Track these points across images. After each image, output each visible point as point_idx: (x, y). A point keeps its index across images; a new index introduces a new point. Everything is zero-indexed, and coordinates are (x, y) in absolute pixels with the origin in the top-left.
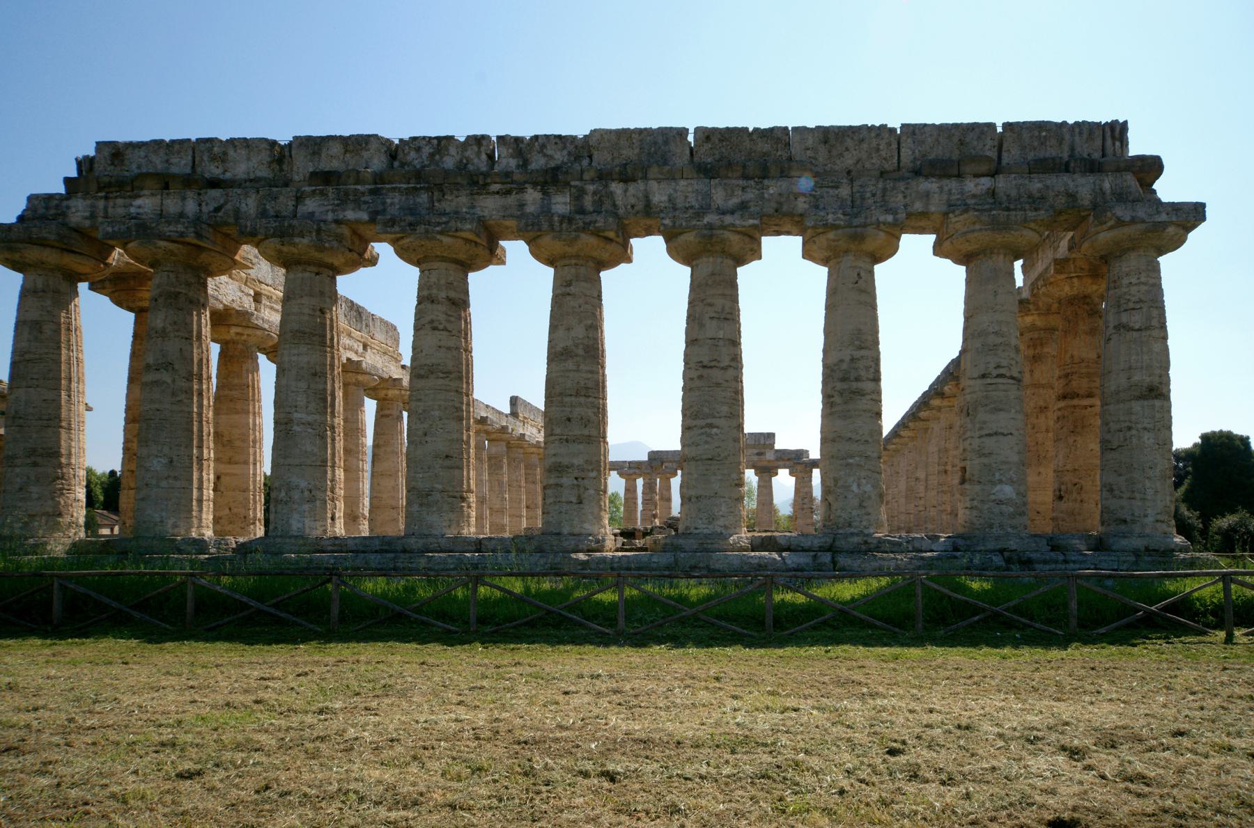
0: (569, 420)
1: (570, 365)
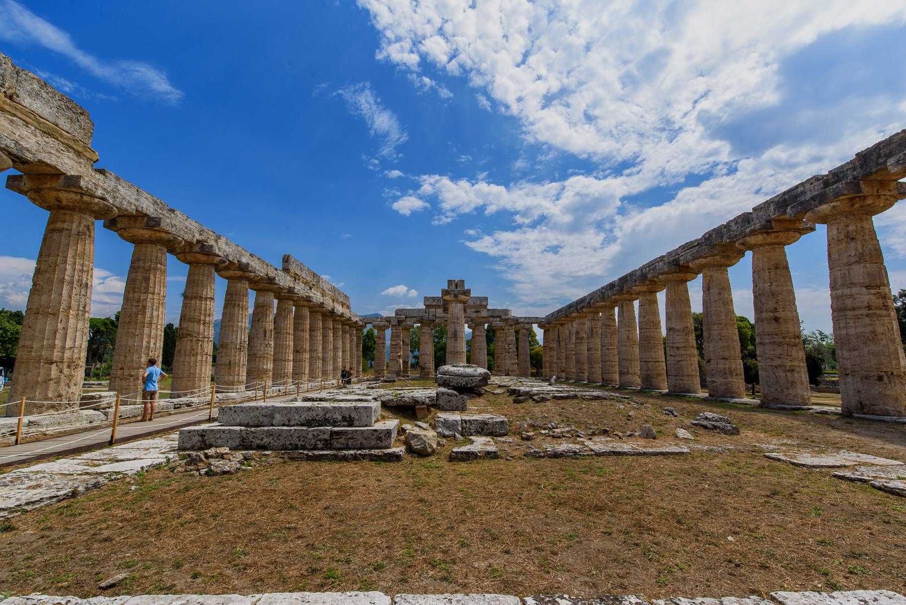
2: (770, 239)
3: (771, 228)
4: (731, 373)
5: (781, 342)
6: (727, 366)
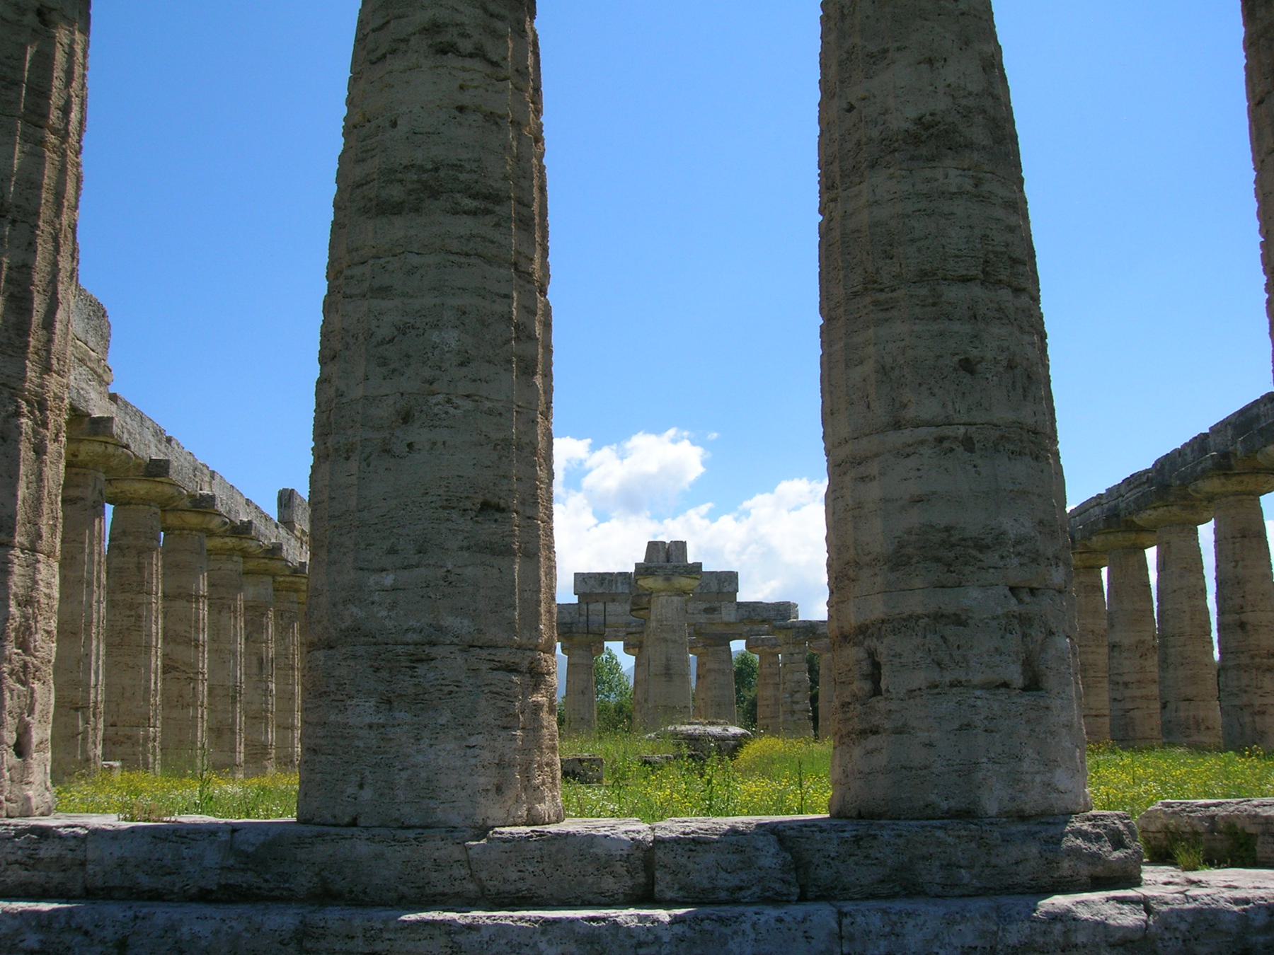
0: (967, 366)
1: (949, 174)
2: (1232, 485)
3: (1230, 468)
4: (1197, 724)
5: (1247, 666)
6: (1191, 714)
